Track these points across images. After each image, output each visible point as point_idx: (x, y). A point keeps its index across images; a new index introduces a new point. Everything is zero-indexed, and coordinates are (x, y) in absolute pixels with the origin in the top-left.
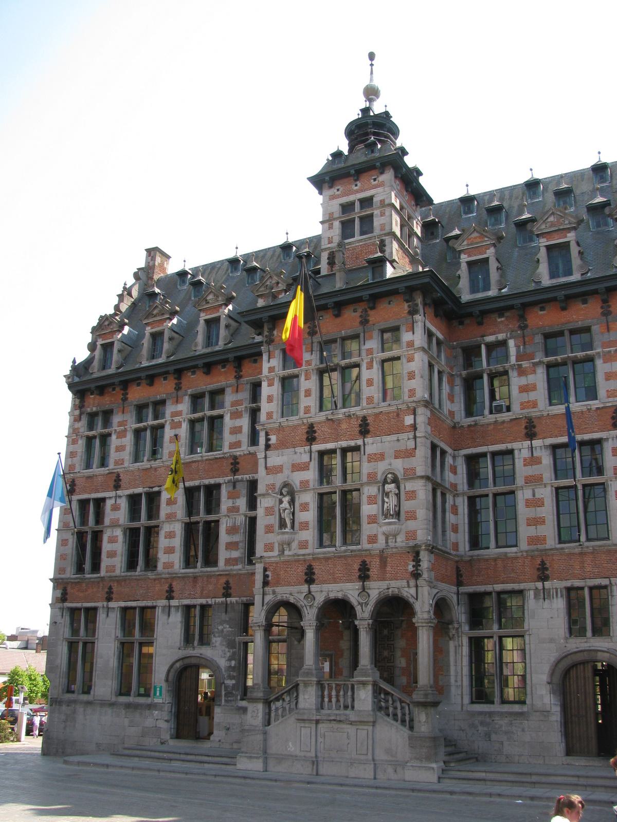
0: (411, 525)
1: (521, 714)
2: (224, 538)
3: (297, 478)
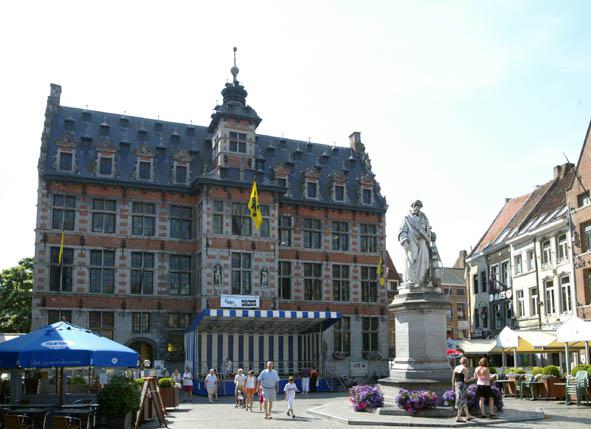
3: (223, 262)
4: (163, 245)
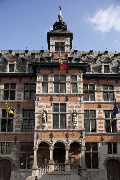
0: (80, 125)
1: (98, 171)
2: (15, 124)
3: (47, 110)
4: (19, 105)
